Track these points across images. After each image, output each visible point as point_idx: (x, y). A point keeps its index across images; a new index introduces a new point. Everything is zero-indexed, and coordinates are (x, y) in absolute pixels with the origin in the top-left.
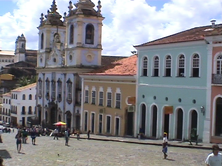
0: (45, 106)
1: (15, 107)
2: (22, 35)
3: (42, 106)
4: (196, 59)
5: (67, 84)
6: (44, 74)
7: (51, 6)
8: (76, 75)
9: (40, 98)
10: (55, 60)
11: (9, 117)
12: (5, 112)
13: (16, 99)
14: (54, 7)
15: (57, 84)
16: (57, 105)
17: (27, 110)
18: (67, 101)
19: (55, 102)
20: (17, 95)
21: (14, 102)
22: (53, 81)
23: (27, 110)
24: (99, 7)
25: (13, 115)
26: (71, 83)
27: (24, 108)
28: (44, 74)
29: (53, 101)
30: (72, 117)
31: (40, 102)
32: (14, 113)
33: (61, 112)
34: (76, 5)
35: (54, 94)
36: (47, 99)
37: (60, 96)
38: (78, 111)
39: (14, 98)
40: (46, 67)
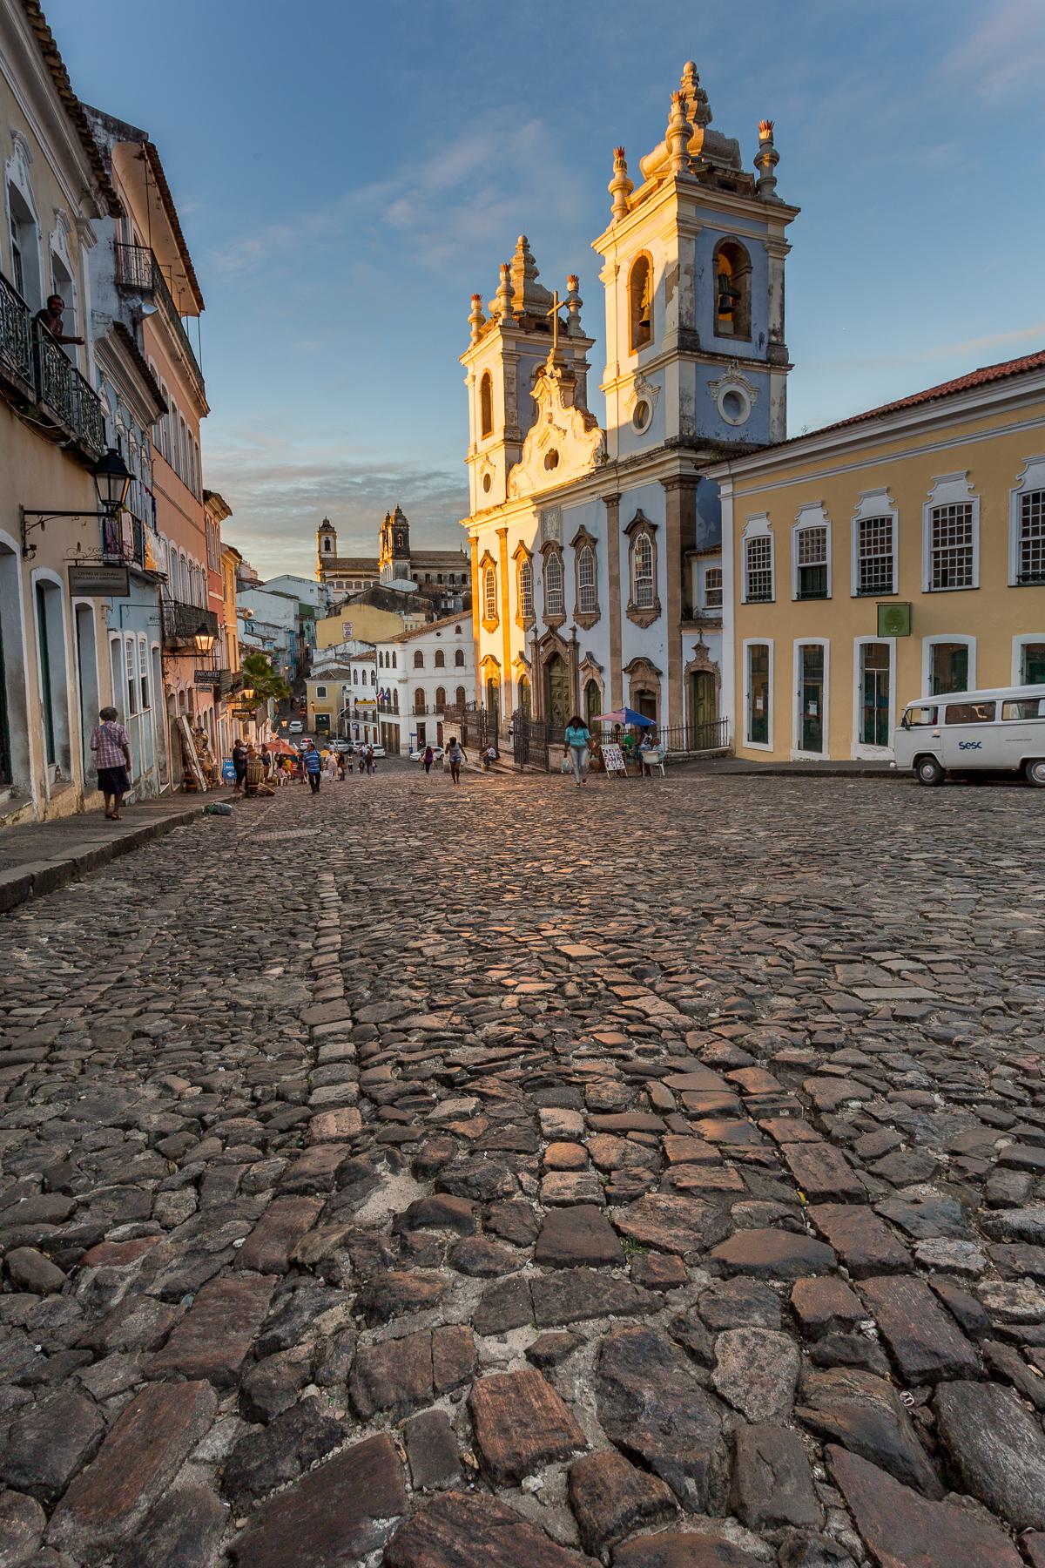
2: (398, 510)
3: (500, 659)
5: (624, 541)
8: (687, 483)
9: (491, 631)
10: (553, 460)
11: (375, 725)
13: (395, 666)
15: (569, 556)
16: (575, 644)
17: (431, 701)
18: (633, 610)
19: (565, 632)
21: (389, 678)
23: (431, 701)
25: (383, 718)
26: (655, 527)
27: (420, 694)
28: (503, 533)
29: (553, 629)
30: (665, 682)
32: (389, 711)
33: (601, 669)
38: (700, 649)
39: (388, 666)
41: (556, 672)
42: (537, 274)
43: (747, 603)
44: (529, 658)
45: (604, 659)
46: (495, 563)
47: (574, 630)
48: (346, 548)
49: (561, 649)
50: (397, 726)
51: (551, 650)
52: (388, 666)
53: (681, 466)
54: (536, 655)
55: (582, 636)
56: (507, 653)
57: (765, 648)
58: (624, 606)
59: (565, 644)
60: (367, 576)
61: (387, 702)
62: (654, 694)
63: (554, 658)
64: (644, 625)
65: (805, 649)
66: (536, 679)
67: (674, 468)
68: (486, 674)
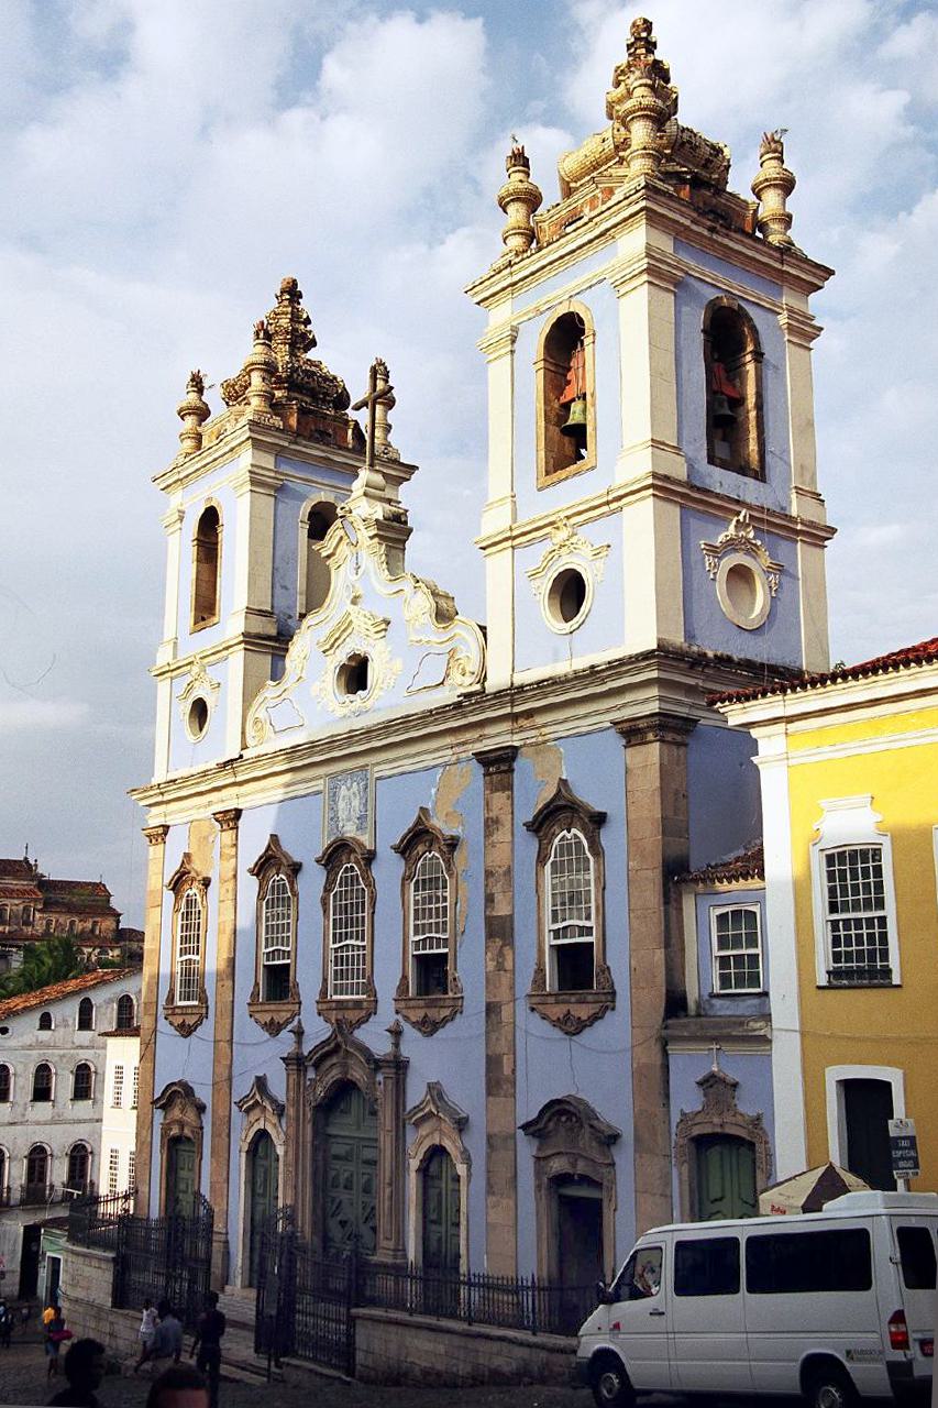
0: (243, 1086)
3: (204, 1094)
9: (186, 1030)
10: (355, 675)
15: (388, 870)
16: (399, 1066)
26: (600, 819)
29: (343, 1029)
30: (624, 1157)
33: (462, 1125)
35: (350, 966)
36: (274, 1028)
37: (432, 972)
41: (344, 1127)
42: (313, 343)
43: (830, 987)
44: (279, 1087)
45: (467, 1095)
46: (206, 883)
47: (396, 1033)
49: (358, 1074)
51: (335, 1074)
53: (661, 699)
54: (298, 1088)
55: (414, 1046)
56: (224, 1082)
57: (884, 1088)
58: (525, 985)
59: (376, 1064)
62: (598, 1185)
63: (344, 1090)
64: (573, 1027)
65: (850, 1088)
66: (294, 1141)
67: (646, 704)
68: (166, 1128)
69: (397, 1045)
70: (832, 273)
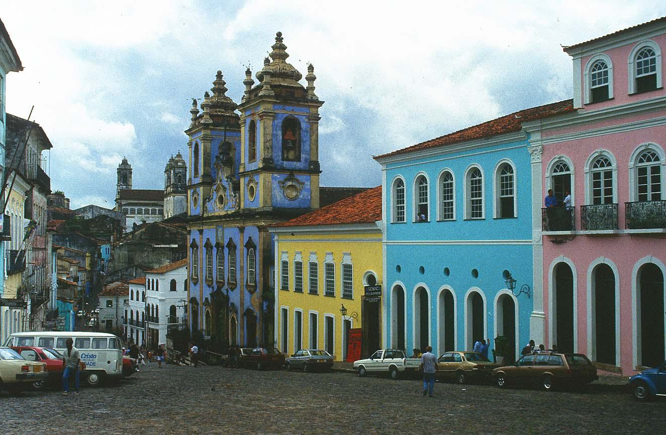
0: (204, 300)
1: (155, 307)
2: (179, 156)
4: (506, 177)
6: (201, 232)
7: (214, 83)
9: (195, 284)
10: (221, 199)
12: (135, 318)
13: (157, 290)
14: (220, 86)
15: (226, 251)
20: (157, 280)
21: (154, 297)
22: (218, 245)
24: (311, 79)
28: (201, 232)
29: (219, 288)
31: (195, 292)
34: (260, 78)
36: (209, 286)
39: (153, 289)
40: (205, 215)
47: (227, 290)
48: (138, 183)
50: (157, 331)
52: (153, 289)
60: (153, 205)
61: (151, 315)
66: (212, 312)
68: (192, 308)
69: (227, 293)
70: (323, 102)
